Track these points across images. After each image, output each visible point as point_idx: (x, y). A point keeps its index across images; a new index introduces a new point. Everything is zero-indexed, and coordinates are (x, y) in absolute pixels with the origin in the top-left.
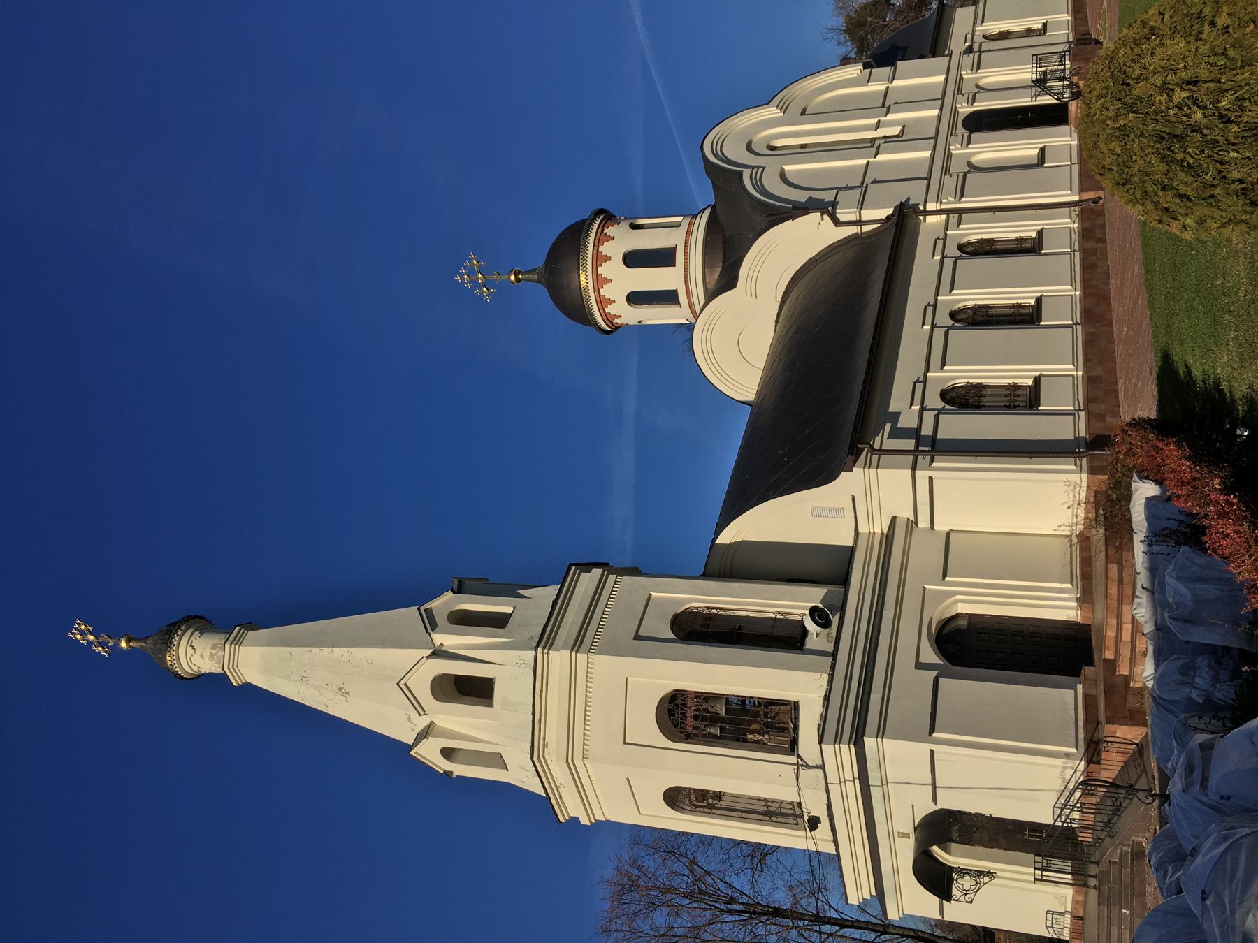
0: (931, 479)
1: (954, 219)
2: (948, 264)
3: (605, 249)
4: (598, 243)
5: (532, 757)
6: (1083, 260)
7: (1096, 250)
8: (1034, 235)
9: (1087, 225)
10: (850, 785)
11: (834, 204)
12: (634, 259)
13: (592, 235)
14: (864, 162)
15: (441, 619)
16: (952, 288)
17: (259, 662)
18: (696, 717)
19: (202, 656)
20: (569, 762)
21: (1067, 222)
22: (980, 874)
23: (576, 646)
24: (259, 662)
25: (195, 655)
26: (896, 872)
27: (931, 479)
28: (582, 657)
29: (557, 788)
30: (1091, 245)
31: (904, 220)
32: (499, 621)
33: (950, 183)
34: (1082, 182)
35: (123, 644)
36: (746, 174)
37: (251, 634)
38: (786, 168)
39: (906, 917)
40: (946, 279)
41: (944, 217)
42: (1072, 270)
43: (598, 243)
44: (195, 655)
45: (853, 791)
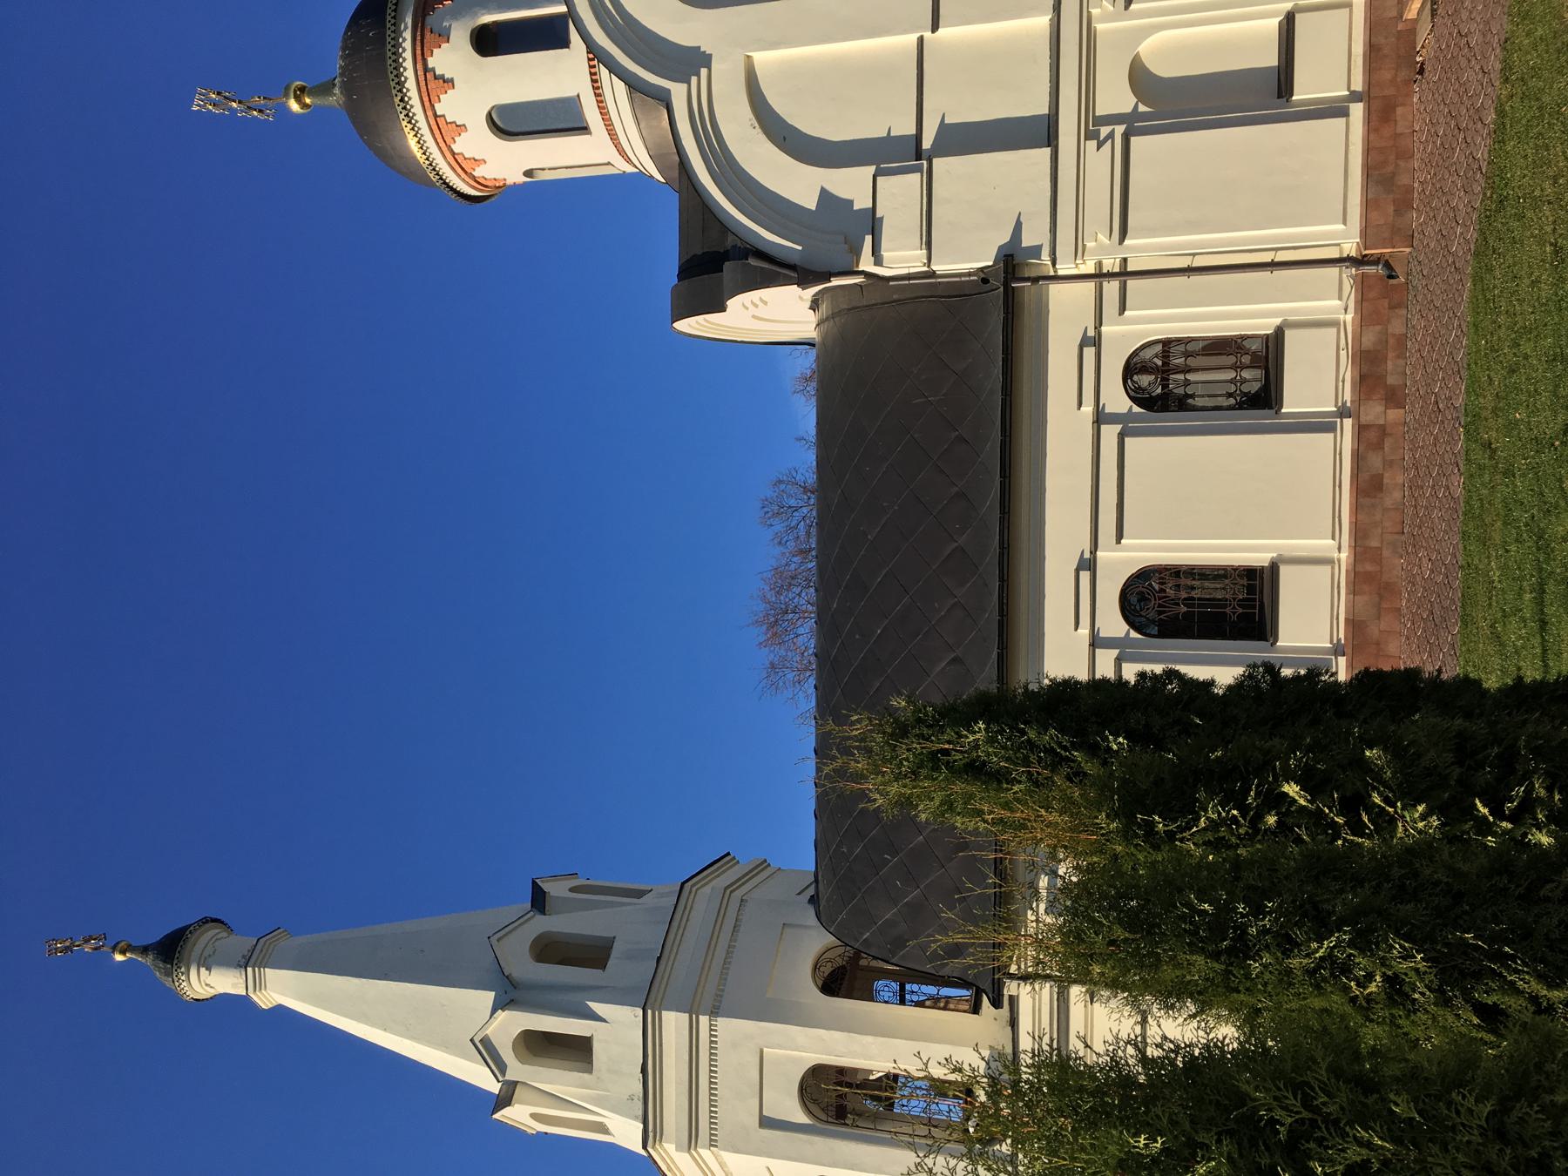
1: (1111, 288)
2: (1110, 433)
3: (447, 105)
4: (428, 103)
6: (1358, 457)
7: (1383, 431)
8: (1266, 326)
9: (1369, 340)
11: (872, 223)
12: (510, 123)
13: (411, 84)
14: (913, 38)
15: (507, 1055)
16: (1120, 536)
21: (1330, 301)
23: (692, 1140)
28: (706, 1153)
30: (1374, 412)
31: (1012, 279)
32: (577, 1051)
33: (1099, 162)
34: (1368, 205)
35: (119, 958)
36: (678, 92)
37: (269, 973)
38: (759, 57)
40: (1110, 513)
41: (1090, 286)
42: (1337, 484)
43: (428, 103)
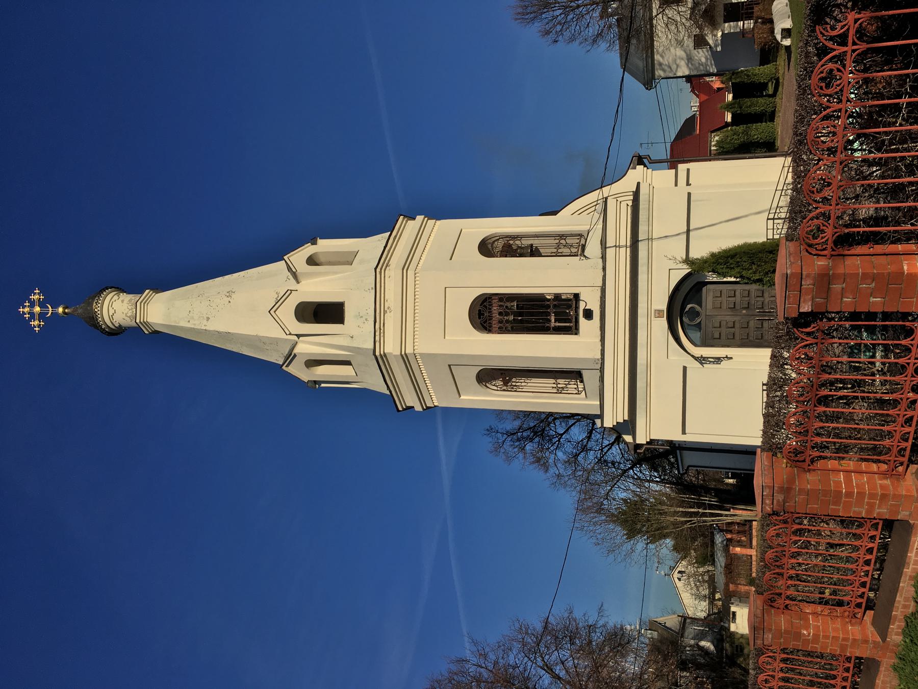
0: (688, 170)
5: (376, 269)
10: (623, 250)
17: (165, 310)
18: (500, 314)
19: (123, 301)
20: (405, 267)
22: (718, 360)
24: (165, 310)
25: (116, 308)
26: (648, 366)
27: (688, 170)
29: (385, 312)
39: (651, 442)
44: (116, 308)
45: (624, 255)
